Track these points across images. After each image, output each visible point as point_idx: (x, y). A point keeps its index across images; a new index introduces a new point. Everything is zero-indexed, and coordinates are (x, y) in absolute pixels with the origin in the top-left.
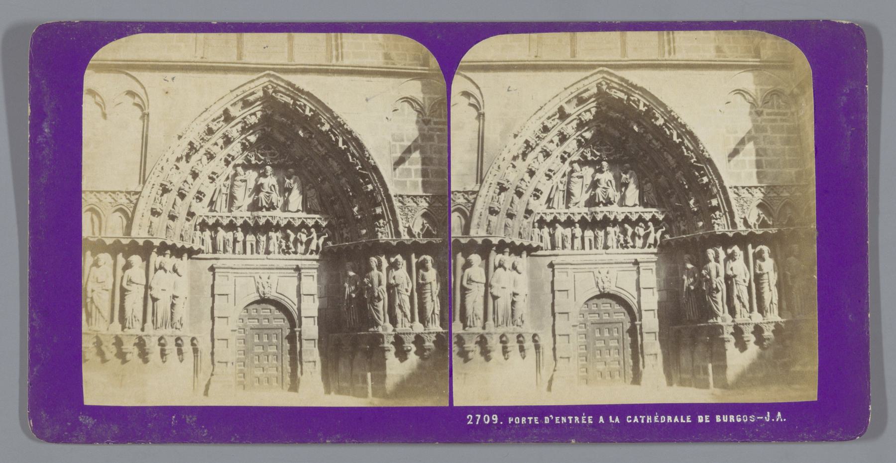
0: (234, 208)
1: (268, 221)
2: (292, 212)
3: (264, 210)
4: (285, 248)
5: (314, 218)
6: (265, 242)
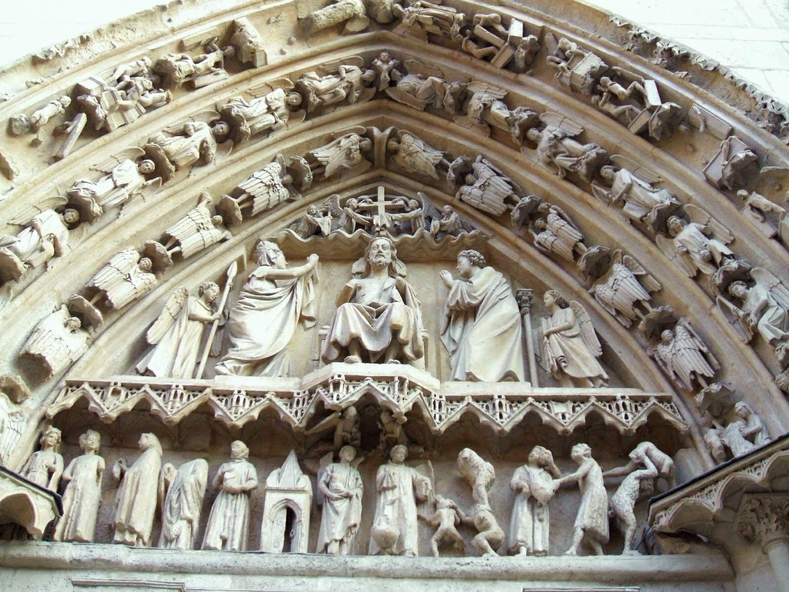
0: (230, 364)
4: (454, 530)
5: (584, 399)
6: (357, 504)
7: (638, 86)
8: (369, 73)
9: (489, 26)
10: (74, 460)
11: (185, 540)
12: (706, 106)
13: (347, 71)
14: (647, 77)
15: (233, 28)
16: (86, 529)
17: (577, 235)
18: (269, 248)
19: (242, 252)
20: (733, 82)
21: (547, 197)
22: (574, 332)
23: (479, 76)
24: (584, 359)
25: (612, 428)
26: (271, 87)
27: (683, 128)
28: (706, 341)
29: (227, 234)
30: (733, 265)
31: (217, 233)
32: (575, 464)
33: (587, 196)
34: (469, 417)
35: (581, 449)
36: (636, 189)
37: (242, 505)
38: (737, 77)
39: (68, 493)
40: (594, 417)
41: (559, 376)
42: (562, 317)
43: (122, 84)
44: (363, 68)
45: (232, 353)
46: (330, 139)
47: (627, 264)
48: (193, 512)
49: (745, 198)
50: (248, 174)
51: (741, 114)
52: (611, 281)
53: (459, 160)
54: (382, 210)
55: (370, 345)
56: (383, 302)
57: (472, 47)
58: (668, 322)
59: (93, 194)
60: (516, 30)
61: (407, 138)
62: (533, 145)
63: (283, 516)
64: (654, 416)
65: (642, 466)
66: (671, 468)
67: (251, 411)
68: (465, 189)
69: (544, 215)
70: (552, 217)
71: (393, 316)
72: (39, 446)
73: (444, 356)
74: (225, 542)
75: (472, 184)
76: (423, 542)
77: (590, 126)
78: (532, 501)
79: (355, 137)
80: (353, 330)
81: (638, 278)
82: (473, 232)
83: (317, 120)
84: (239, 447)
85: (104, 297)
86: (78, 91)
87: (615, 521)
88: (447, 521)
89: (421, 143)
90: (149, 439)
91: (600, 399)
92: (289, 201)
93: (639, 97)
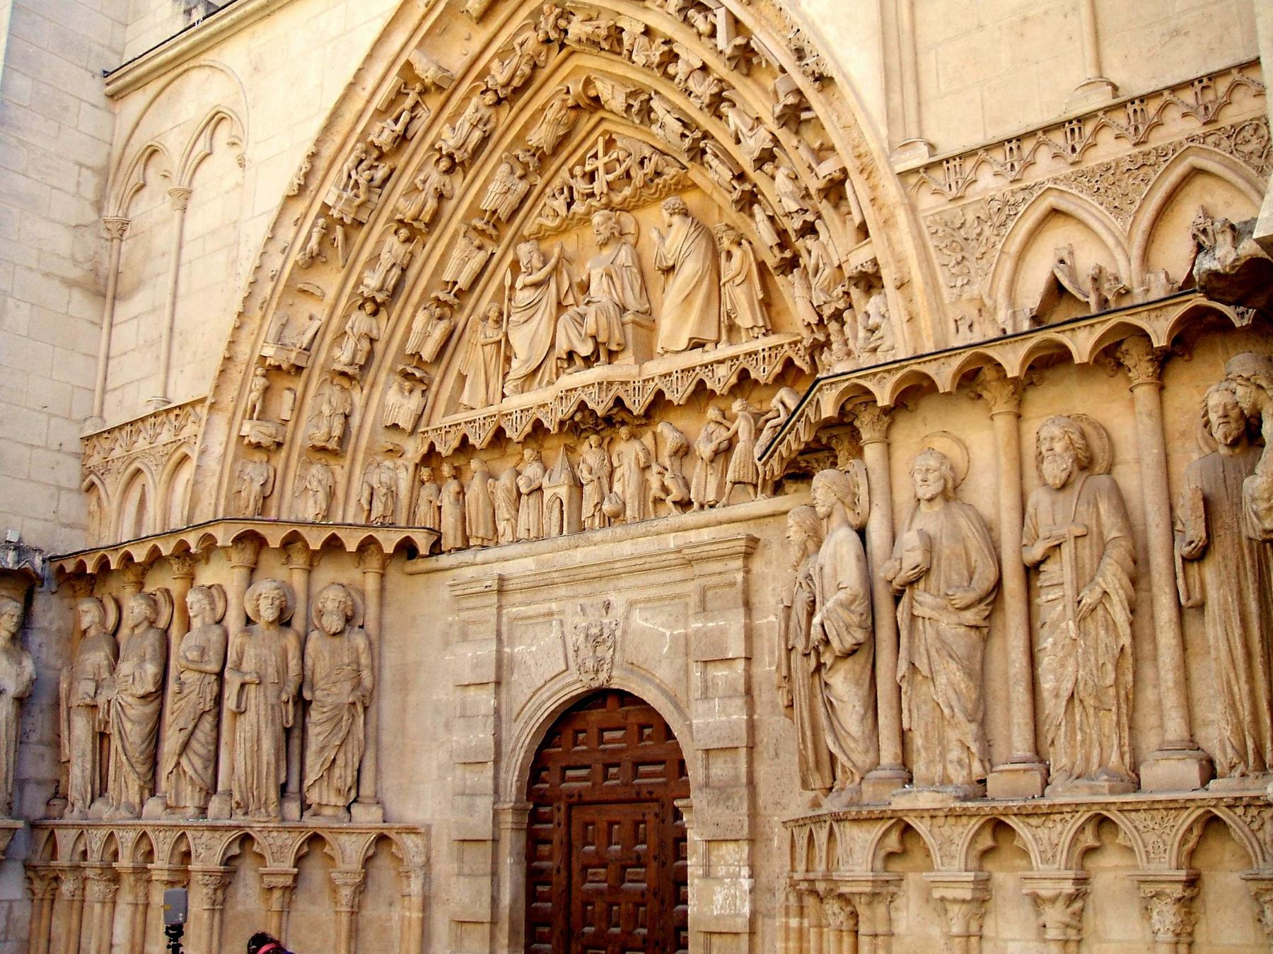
13: (522, 45)
21: (706, 135)
22: (738, 280)
26: (467, 98)
43: (352, 182)
86: (326, 207)
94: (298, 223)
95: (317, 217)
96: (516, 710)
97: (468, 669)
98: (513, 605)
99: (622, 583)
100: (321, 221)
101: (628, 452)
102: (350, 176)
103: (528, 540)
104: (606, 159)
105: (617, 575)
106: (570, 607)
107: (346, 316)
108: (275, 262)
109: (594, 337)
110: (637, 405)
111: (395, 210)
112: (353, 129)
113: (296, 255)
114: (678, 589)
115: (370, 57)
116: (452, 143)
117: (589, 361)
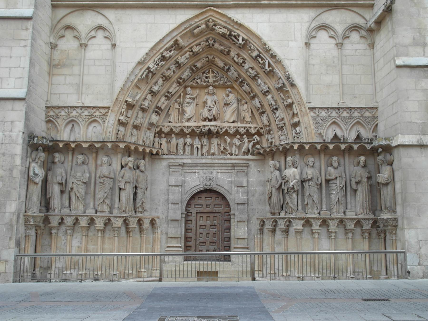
1: (209, 130)
2: (229, 122)
3: (207, 121)
4: (223, 150)
5: (246, 127)
7: (265, 62)
8: (207, 43)
9: (235, 36)
10: (161, 139)
11: (182, 153)
12: (277, 70)
14: (267, 60)
15: (177, 40)
16: (166, 152)
17: (249, 90)
18: (189, 89)
19: (183, 89)
20: (283, 65)
23: (232, 47)
24: (248, 117)
25: (251, 133)
26: (186, 52)
27: (272, 73)
28: (269, 118)
29: (180, 87)
30: (274, 107)
31: (178, 88)
32: (244, 139)
33: (252, 81)
34: (226, 131)
35: (245, 136)
36: (261, 85)
37: (190, 147)
38: (284, 65)
39: (162, 146)
40: (248, 131)
41: (243, 120)
42: (245, 106)
43: (157, 63)
44: (206, 42)
45: (185, 117)
46: (199, 60)
47: (258, 99)
48: (182, 149)
49: (279, 94)
50: (183, 73)
51: (283, 73)
52: (255, 101)
53: (227, 67)
54: (211, 77)
55: (210, 118)
56: (212, 106)
57: (231, 40)
58: (263, 113)
59: (156, 90)
60: (240, 41)
61: (216, 59)
62: (243, 67)
63: (197, 149)
64: (258, 130)
65: (254, 140)
66: (259, 141)
67: (190, 130)
68: (229, 73)
69: (244, 83)
70: (245, 85)
71: (213, 113)
72: (155, 137)
73: (223, 113)
74: (188, 153)
75: (230, 72)
76: (218, 152)
77: (255, 66)
78: (236, 145)
79: (205, 59)
80: (207, 116)
81: (260, 102)
82: (230, 83)
83: (196, 56)
84: (188, 136)
85: (160, 107)
86: (149, 68)
87: (249, 150)
88: (222, 149)
89: (219, 60)
90: (173, 135)
91: (249, 127)
92: (192, 75)
93: (264, 64)
94: (141, 70)
95: (147, 69)
96: (186, 192)
97: (173, 182)
98: (185, 169)
99: (215, 168)
100: (147, 71)
101: (215, 141)
102: (156, 62)
103: (187, 155)
104: (212, 75)
105: (215, 166)
106: (201, 172)
107: (147, 95)
108: (132, 78)
109: (214, 116)
110: (222, 131)
111: (163, 73)
112: (159, 50)
113: (139, 77)
114: (230, 171)
115: (167, 35)
116: (182, 61)
117: (210, 120)
